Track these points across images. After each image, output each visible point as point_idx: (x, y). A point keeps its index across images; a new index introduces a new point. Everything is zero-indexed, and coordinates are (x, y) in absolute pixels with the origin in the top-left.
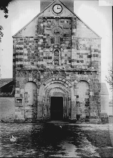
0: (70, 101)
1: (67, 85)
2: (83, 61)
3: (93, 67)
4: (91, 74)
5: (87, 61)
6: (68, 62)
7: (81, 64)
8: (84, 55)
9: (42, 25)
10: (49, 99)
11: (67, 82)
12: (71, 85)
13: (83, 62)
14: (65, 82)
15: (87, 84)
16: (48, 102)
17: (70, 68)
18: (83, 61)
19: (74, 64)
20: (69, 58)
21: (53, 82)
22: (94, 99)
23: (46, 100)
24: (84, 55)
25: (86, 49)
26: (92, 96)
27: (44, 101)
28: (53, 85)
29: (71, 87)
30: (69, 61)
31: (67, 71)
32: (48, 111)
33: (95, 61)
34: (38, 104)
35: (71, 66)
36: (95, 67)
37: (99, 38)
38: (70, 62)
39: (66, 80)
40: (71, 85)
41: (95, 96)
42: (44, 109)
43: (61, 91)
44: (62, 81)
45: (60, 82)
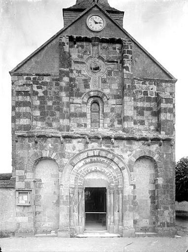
0: (121, 195)
1: (117, 165)
2: (144, 121)
3: (163, 131)
4: (160, 145)
5: (151, 121)
6: (116, 123)
7: (141, 127)
8: (145, 112)
9: (42, 210)
10: (82, 192)
11: (116, 160)
12: (123, 165)
13: (144, 124)
14: (112, 160)
15: (152, 164)
16: (80, 196)
17: (121, 133)
18: (144, 121)
19: (126, 125)
20: (119, 115)
21: (88, 160)
22: (165, 191)
23: (76, 193)
24: (145, 112)
25: (149, 100)
26: (162, 186)
27: (72, 195)
28: (88, 165)
29: (124, 168)
30: (118, 121)
31: (115, 139)
32: (80, 214)
33: (167, 121)
34: (61, 201)
35: (124, 130)
36: (167, 131)
37: (171, 80)
38: (120, 122)
39: (114, 155)
40: (123, 165)
41: (167, 185)
42: (72, 211)
43: (103, 177)
44: (106, 157)
45: (102, 159)
